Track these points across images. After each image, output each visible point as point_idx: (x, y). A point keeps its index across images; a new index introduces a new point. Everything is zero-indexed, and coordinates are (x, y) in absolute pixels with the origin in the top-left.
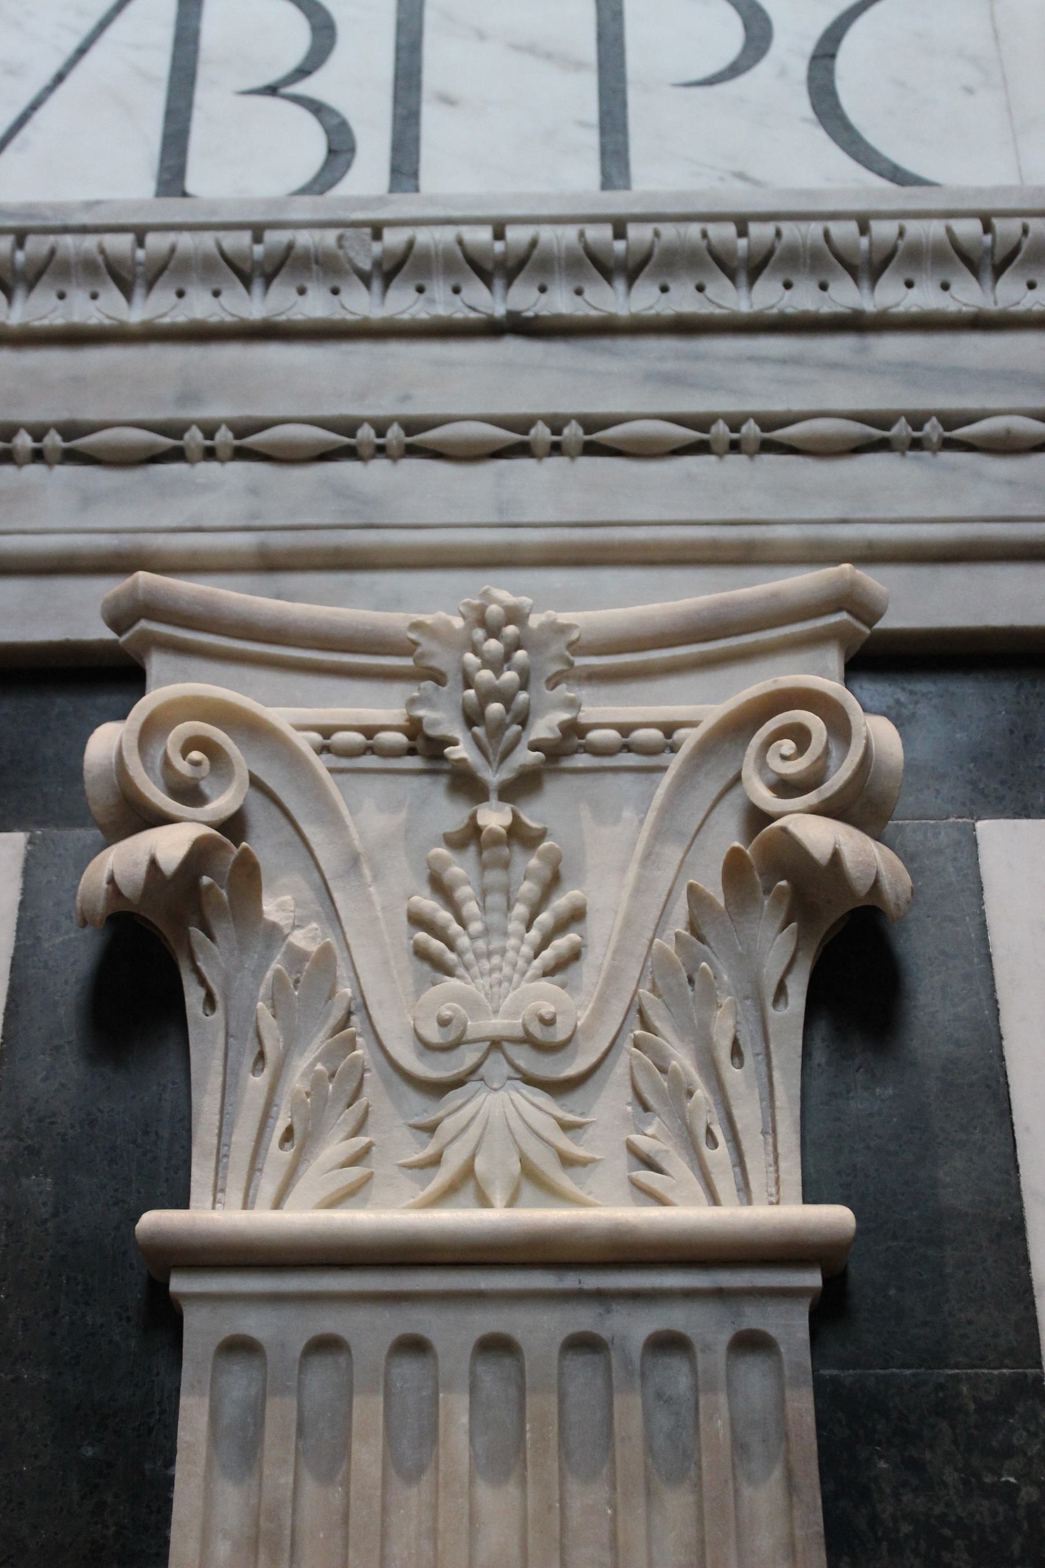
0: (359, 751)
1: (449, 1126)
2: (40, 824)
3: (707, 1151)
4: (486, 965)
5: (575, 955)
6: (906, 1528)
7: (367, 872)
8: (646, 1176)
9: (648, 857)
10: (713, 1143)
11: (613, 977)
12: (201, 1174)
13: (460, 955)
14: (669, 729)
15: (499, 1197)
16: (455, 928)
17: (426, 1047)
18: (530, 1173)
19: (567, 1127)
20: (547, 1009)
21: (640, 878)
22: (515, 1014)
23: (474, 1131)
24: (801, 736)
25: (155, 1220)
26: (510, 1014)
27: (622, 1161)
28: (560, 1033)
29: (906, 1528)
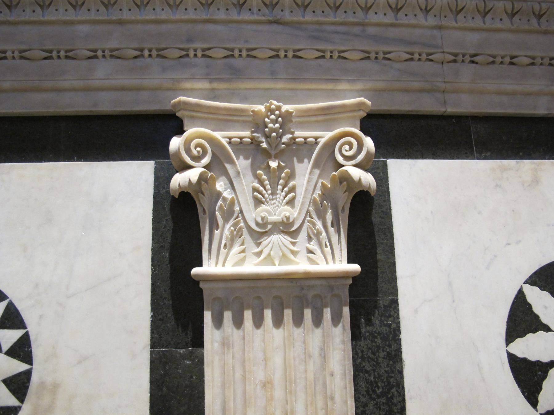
0: (240, 146)
1: (264, 243)
2: (157, 159)
3: (325, 249)
4: (272, 202)
5: (294, 198)
6: (367, 334)
7: (242, 176)
9: (311, 172)
10: (326, 246)
11: (303, 204)
12: (205, 255)
13: (266, 199)
14: (316, 139)
15: (277, 263)
16: (264, 192)
17: (257, 224)
18: (284, 255)
19: (293, 244)
20: (287, 214)
21: (309, 178)
22: (279, 215)
23: (270, 245)
24: (351, 145)
25: (195, 271)
26: (279, 215)
27: (305, 251)
28: (291, 221)
29: (367, 334)
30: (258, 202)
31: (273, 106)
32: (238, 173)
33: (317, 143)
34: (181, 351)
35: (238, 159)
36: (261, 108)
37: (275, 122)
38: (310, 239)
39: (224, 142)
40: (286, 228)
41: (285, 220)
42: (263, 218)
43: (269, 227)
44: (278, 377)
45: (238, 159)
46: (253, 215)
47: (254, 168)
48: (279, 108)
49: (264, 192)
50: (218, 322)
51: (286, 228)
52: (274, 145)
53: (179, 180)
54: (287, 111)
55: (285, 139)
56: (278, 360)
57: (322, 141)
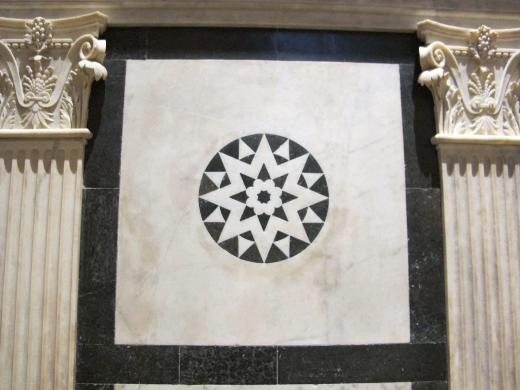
8: (505, 130)
9: (506, 76)
14: (509, 53)
17: (473, 108)
19: (495, 123)
20: (493, 103)
23: (481, 123)
26: (487, 102)
27: (502, 128)
30: (472, 94)
31: (484, 30)
32: (459, 75)
33: (509, 57)
34: (426, 190)
35: (459, 64)
36: (476, 31)
37: (486, 40)
38: (505, 120)
39: (451, 52)
40: (490, 111)
41: (491, 106)
42: (477, 105)
43: (481, 111)
44: (488, 206)
45: (459, 64)
46: (469, 103)
47: (469, 72)
48: (488, 31)
49: (477, 88)
50: (450, 171)
51: (490, 111)
52: (484, 56)
53: (426, 76)
54: (493, 34)
55: (491, 52)
56: (487, 197)
57: (513, 56)
